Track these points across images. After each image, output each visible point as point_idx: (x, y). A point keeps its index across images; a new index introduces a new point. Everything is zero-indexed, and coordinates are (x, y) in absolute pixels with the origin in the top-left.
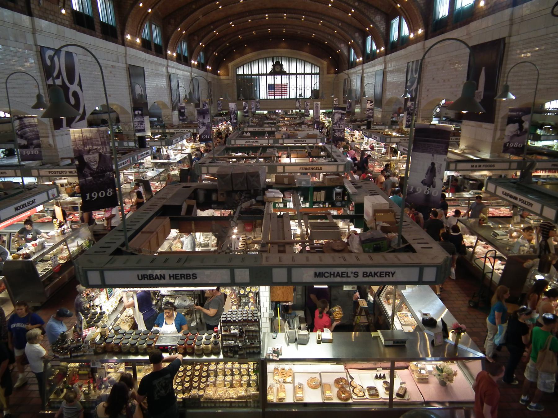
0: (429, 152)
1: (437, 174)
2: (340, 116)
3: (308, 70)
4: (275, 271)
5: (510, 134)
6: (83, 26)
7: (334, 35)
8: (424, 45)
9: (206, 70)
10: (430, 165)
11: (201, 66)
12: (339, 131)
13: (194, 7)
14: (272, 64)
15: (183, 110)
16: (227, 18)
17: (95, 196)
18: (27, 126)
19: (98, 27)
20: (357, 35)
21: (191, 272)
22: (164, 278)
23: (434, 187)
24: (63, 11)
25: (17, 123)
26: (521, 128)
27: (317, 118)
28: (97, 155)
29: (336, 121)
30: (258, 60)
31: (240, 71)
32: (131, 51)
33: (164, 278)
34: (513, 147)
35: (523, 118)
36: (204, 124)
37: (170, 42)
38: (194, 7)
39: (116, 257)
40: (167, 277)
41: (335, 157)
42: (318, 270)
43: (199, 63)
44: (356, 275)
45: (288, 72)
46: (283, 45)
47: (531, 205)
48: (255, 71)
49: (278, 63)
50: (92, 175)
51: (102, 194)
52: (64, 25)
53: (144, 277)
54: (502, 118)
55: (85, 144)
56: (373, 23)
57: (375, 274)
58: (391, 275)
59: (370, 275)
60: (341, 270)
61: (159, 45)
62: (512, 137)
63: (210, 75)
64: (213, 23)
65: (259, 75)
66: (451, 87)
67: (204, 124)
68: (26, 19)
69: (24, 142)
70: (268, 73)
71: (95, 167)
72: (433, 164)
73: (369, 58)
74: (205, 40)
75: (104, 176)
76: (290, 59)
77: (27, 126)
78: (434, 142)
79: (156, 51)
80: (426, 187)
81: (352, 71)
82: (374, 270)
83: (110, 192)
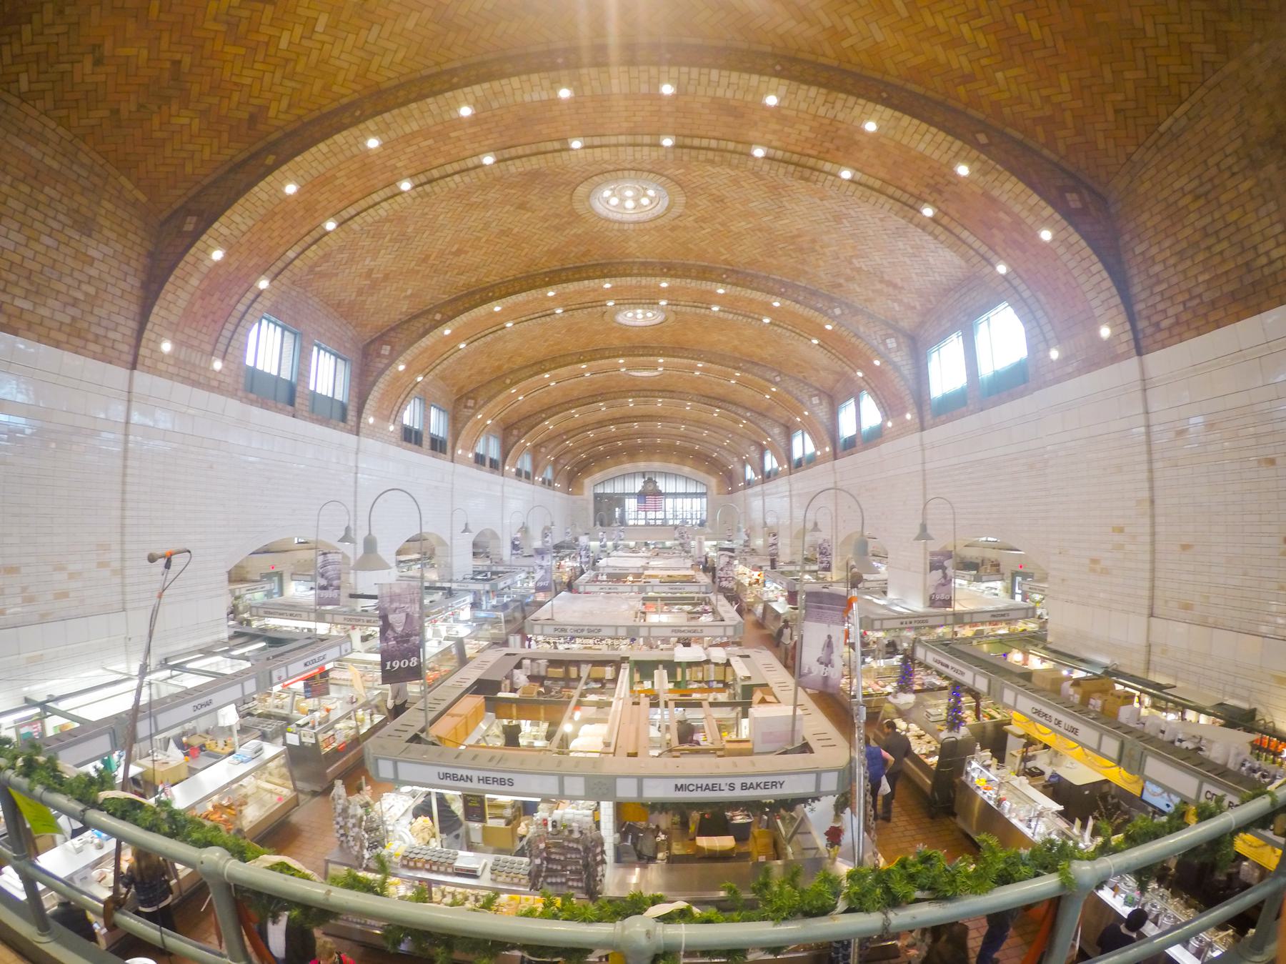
0: (824, 622)
1: (835, 650)
2: (727, 559)
4: (620, 782)
5: (935, 584)
6: (410, 441)
7: (723, 447)
8: (833, 466)
9: (554, 489)
10: (826, 638)
11: (547, 483)
13: (544, 416)
15: (517, 543)
16: (585, 428)
17: (396, 665)
18: (330, 564)
19: (426, 442)
20: (753, 448)
21: (506, 776)
22: (471, 781)
23: (832, 666)
24: (392, 428)
25: (320, 559)
26: (945, 576)
28: (403, 616)
30: (624, 476)
31: (600, 490)
32: (460, 468)
33: (471, 781)
34: (940, 600)
35: (946, 563)
36: (541, 567)
37: (509, 456)
38: (544, 416)
39: (414, 745)
40: (475, 779)
41: (723, 614)
42: (680, 782)
43: (544, 479)
44: (732, 787)
47: (962, 674)
48: (618, 487)
49: (650, 479)
50: (395, 638)
51: (404, 664)
52: (390, 443)
53: (446, 776)
55: (391, 601)
56: (770, 436)
57: (758, 785)
58: (778, 785)
59: (751, 786)
60: (710, 782)
61: (495, 461)
62: (937, 587)
63: (558, 494)
64: (567, 432)
65: (624, 494)
67: (541, 567)
68: (354, 438)
69: (323, 582)
71: (399, 629)
72: (829, 637)
73: (768, 477)
74: (554, 452)
75: (408, 641)
76: (666, 475)
77: (330, 564)
78: (829, 609)
79: (491, 467)
80: (823, 666)
81: (750, 491)
82: (755, 780)
83: (414, 661)
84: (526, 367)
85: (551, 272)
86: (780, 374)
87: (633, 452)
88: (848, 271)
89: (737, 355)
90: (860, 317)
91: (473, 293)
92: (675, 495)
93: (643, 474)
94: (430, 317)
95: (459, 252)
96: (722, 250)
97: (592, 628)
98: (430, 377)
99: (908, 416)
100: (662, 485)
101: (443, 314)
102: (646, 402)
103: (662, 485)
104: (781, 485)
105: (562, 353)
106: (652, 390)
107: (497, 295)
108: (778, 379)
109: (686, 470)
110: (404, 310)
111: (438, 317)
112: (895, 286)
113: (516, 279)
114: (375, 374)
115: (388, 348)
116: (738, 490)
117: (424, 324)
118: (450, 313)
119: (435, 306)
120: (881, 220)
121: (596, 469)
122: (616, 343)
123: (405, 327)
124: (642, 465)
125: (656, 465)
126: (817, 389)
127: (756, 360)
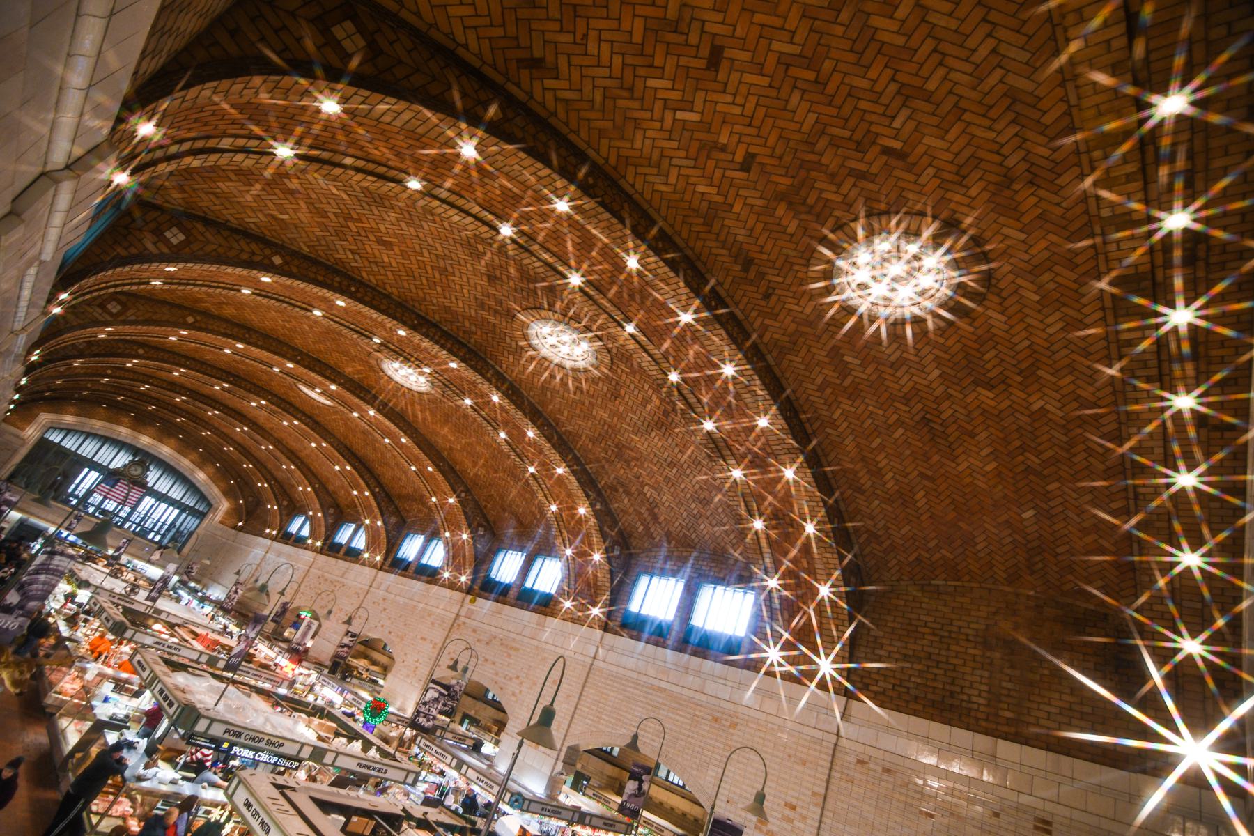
3: (190, 501)
12: (426, 716)
13: (141, 351)
14: (131, 458)
20: (331, 511)
26: (640, 788)
27: (298, 644)
29: (426, 699)
30: (105, 440)
35: (644, 777)
45: (150, 485)
46: (173, 441)
54: (569, 748)
66: (497, 674)
70: (111, 466)
76: (168, 469)
84: (226, 321)
85: (423, 318)
86: (468, 491)
87: (141, 421)
88: (634, 489)
89: (445, 454)
90: (608, 519)
91: (337, 272)
92: (161, 497)
93: (135, 450)
94: (267, 252)
95: (389, 245)
96: (566, 413)
97: (274, 739)
98: (166, 287)
99: (596, 611)
100: (153, 476)
101: (286, 263)
102: (273, 412)
103: (153, 476)
104: (359, 575)
105: (281, 338)
106: (297, 409)
107: (359, 295)
108: (463, 495)
109: (200, 477)
110: (248, 220)
111: (277, 260)
112: (655, 518)
113: (388, 296)
114: (133, 251)
115: (182, 237)
116: (261, 534)
117: (254, 253)
118: (295, 270)
119: (283, 247)
120: (701, 488)
121: (72, 409)
122: (348, 370)
123: (226, 233)
124: (145, 441)
125: (165, 451)
126: (487, 521)
127: (458, 468)
